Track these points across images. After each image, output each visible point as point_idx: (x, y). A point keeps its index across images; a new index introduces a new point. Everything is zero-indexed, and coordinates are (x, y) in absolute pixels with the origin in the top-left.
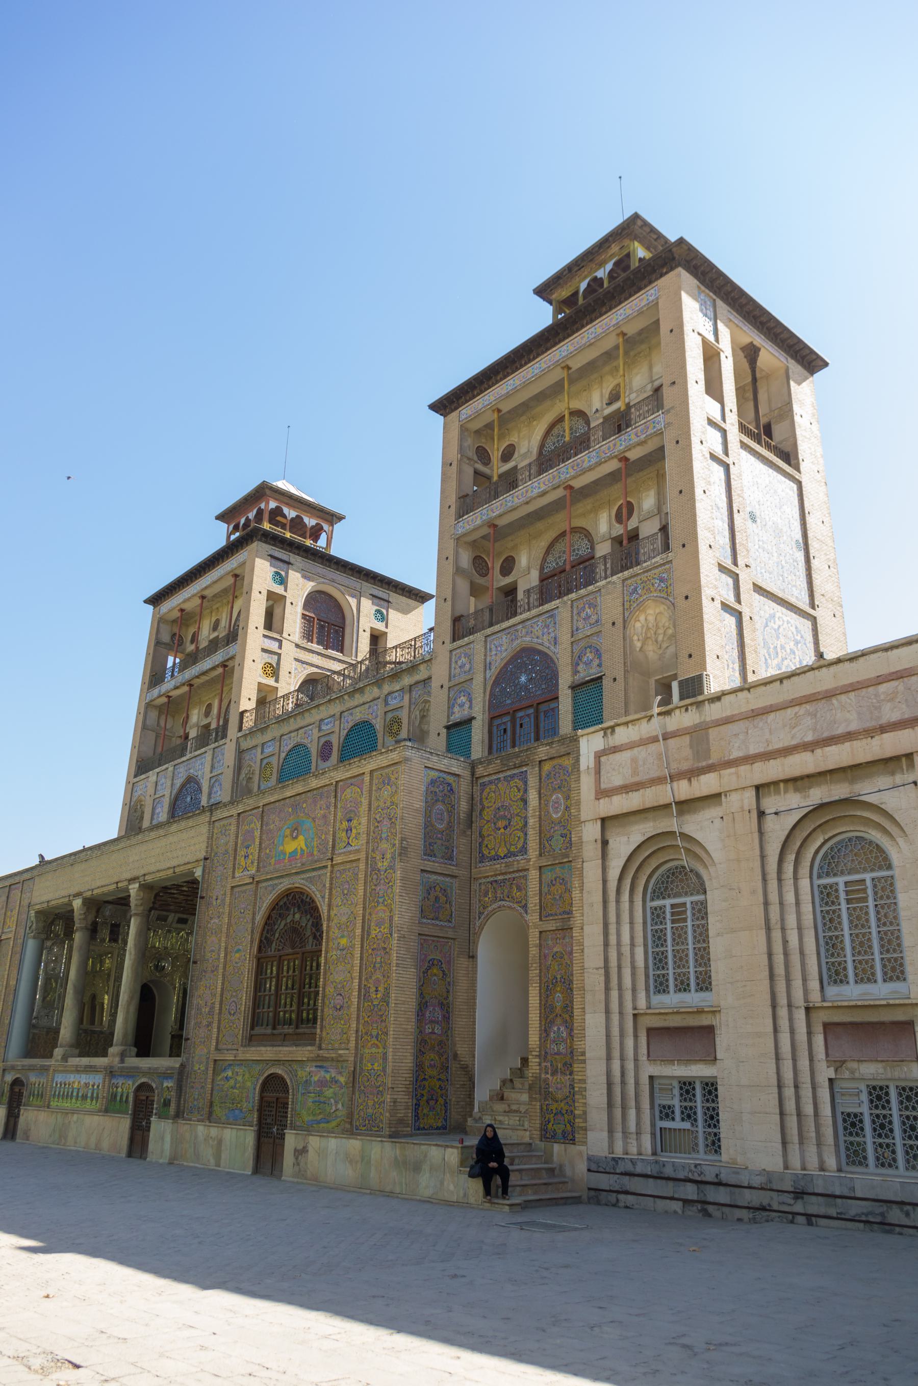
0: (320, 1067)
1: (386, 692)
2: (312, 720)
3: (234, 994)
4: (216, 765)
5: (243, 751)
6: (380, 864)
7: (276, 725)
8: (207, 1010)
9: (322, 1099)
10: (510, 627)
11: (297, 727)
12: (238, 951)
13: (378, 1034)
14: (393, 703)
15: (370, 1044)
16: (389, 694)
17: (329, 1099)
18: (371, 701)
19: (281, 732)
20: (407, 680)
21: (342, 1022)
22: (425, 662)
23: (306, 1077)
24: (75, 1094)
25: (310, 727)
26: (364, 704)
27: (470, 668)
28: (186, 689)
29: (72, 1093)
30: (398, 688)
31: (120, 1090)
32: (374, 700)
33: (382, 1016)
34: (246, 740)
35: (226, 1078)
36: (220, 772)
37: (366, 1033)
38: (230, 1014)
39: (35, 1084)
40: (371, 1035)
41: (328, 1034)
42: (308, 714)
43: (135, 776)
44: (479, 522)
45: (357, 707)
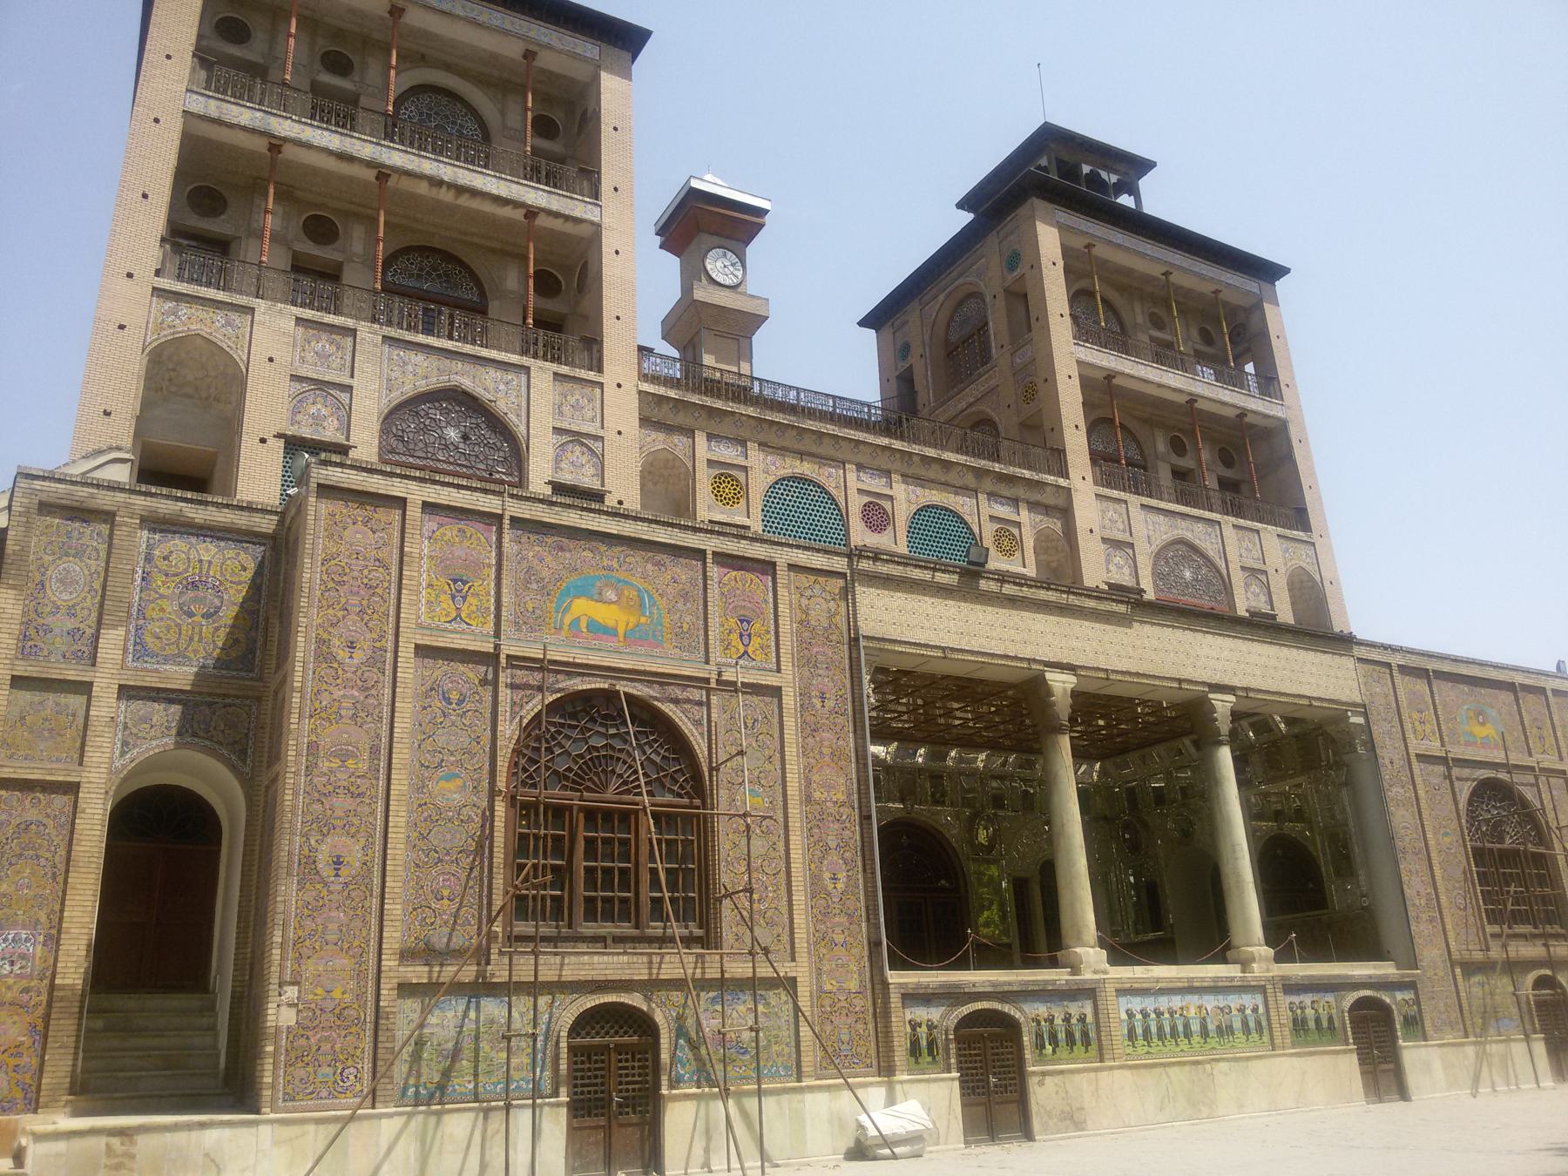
2: (839, 455)
4: (566, 409)
7: (754, 423)
8: (1423, 902)
11: (803, 448)
20: (1021, 492)
22: (1056, 486)
24: (1195, 1027)
27: (1124, 531)
28: (370, 175)
29: (1187, 1026)
30: (1009, 495)
31: (1309, 1012)
39: (1050, 1020)
43: (158, 273)
44: (1105, 363)
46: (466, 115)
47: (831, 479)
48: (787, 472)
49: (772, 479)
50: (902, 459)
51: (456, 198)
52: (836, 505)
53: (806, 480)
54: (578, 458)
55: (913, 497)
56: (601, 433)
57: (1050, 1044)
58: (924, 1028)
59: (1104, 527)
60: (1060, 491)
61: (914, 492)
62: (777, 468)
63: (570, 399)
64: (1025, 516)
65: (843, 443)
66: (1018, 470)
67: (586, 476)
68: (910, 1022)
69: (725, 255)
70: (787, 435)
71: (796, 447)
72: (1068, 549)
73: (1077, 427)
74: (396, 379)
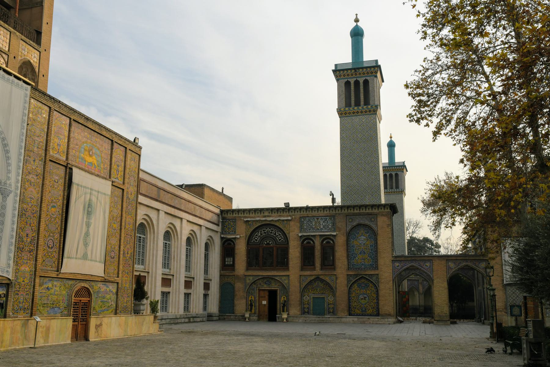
0: (104, 285)
3: (51, 234)
6: (130, 197)
8: (29, 240)
9: (105, 300)
12: (54, 207)
13: (128, 272)
15: (125, 276)
17: (108, 300)
21: (114, 264)
23: (98, 289)
33: (129, 264)
35: (47, 288)
37: (124, 271)
38: (49, 247)
40: (125, 272)
41: (108, 269)
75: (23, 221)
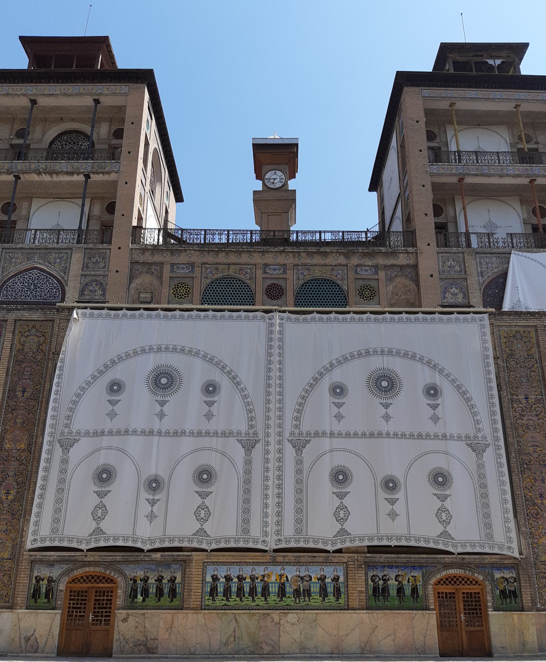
1: (356, 264)
2: (253, 261)
5: (137, 262)
10: (499, 253)
11: (229, 261)
14: (364, 273)
16: (358, 265)
18: (335, 266)
19: (204, 260)
20: (381, 261)
25: (248, 267)
26: (326, 265)
27: (461, 271)
30: (370, 264)
32: (340, 265)
34: (143, 254)
36: (101, 273)
42: (248, 255)
45: (315, 265)
46: (84, 139)
47: (247, 275)
48: (220, 275)
49: (208, 281)
50: (294, 257)
51: (52, 178)
52: (250, 289)
53: (231, 278)
54: (94, 287)
55: (301, 276)
56: (107, 273)
57: (142, 595)
58: (46, 581)
59: (444, 271)
60: (410, 255)
61: (302, 273)
62: (213, 275)
63: (94, 260)
64: (382, 275)
65: (254, 255)
66: (375, 248)
67: (98, 296)
68: (36, 577)
69: (275, 173)
70: (219, 256)
71: (225, 262)
72: (416, 289)
73: (426, 214)
74: (6, 266)
75: (528, 477)
